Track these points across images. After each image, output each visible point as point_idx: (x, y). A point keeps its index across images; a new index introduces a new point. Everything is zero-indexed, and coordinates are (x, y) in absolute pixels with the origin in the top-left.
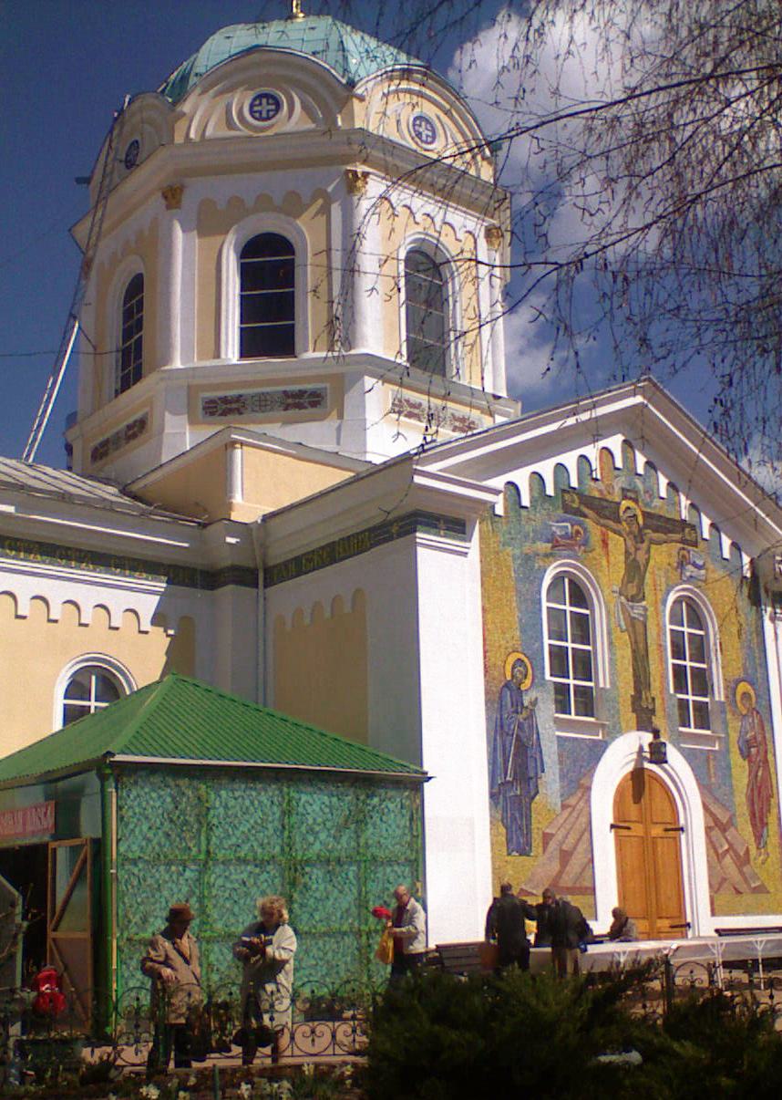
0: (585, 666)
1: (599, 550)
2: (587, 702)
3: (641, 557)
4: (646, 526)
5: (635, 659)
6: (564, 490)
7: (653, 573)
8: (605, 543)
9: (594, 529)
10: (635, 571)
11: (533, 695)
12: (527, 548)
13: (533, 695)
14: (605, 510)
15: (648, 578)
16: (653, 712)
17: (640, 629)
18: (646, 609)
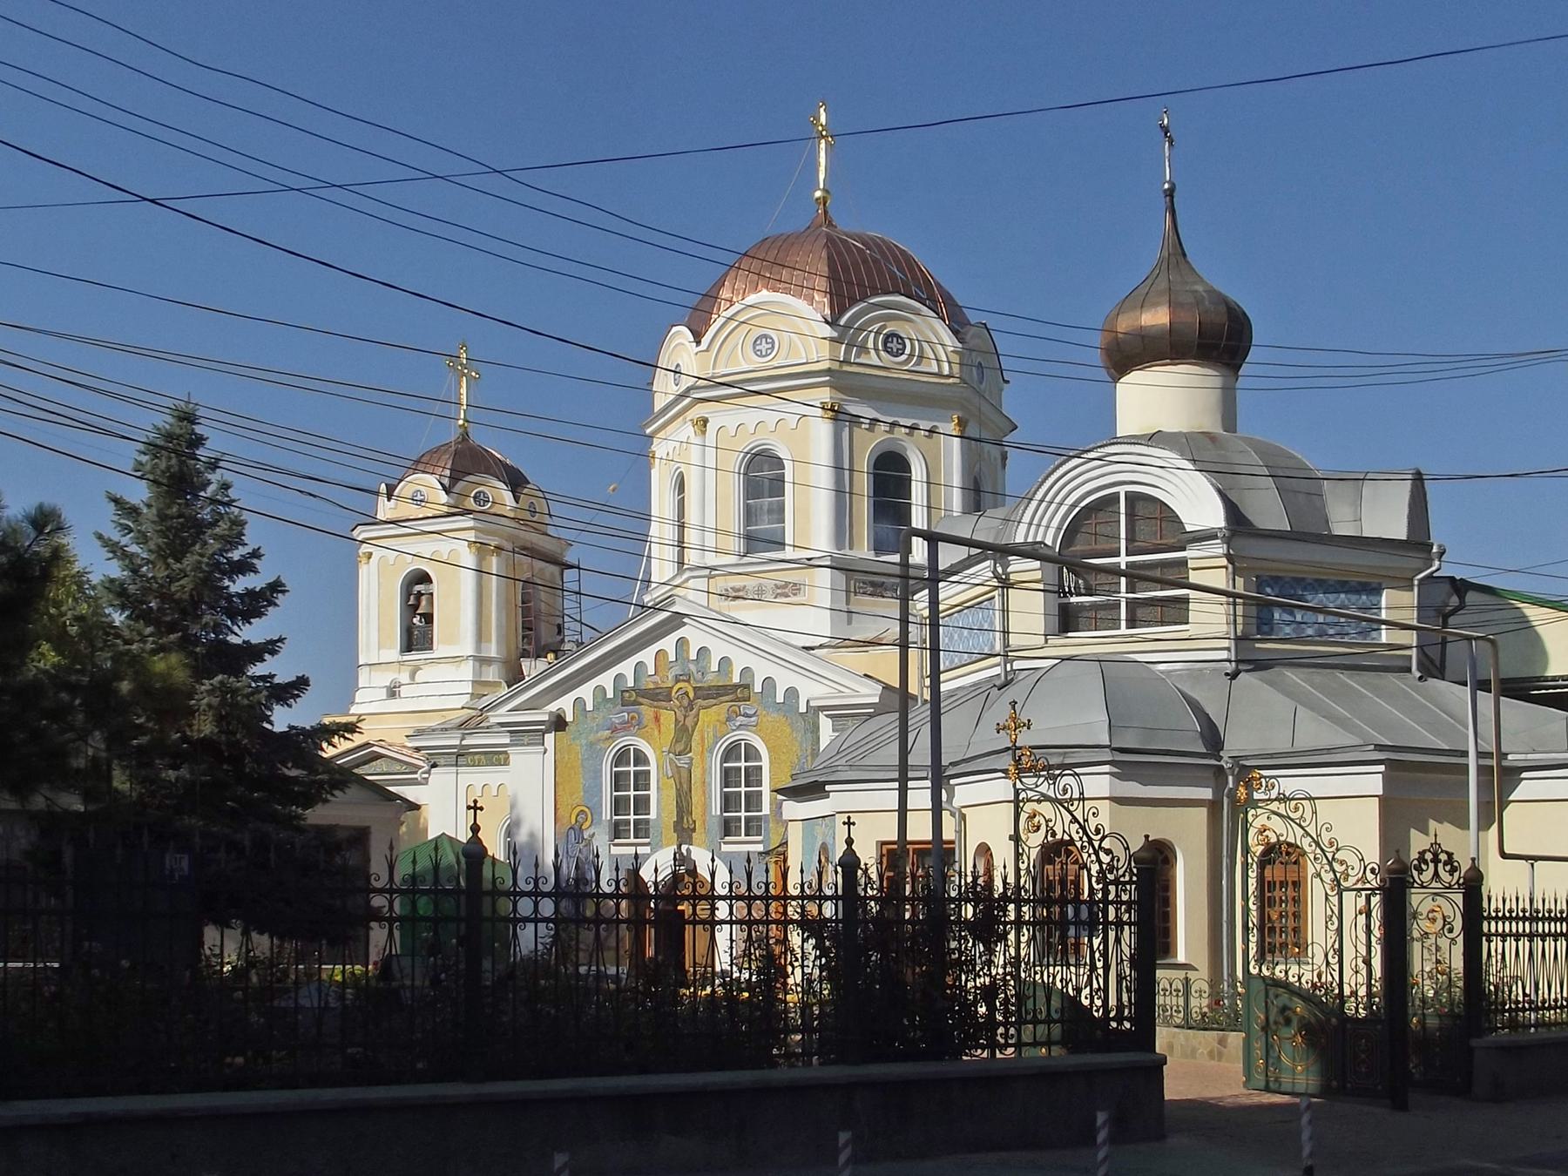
0: (642, 804)
1: (652, 725)
2: (642, 829)
3: (689, 722)
4: (696, 697)
5: (679, 796)
6: (621, 691)
7: (702, 731)
8: (657, 719)
9: (647, 711)
10: (684, 733)
11: (591, 831)
12: (592, 738)
13: (591, 831)
14: (658, 696)
15: (696, 736)
16: (694, 830)
17: (684, 774)
18: (691, 759)
